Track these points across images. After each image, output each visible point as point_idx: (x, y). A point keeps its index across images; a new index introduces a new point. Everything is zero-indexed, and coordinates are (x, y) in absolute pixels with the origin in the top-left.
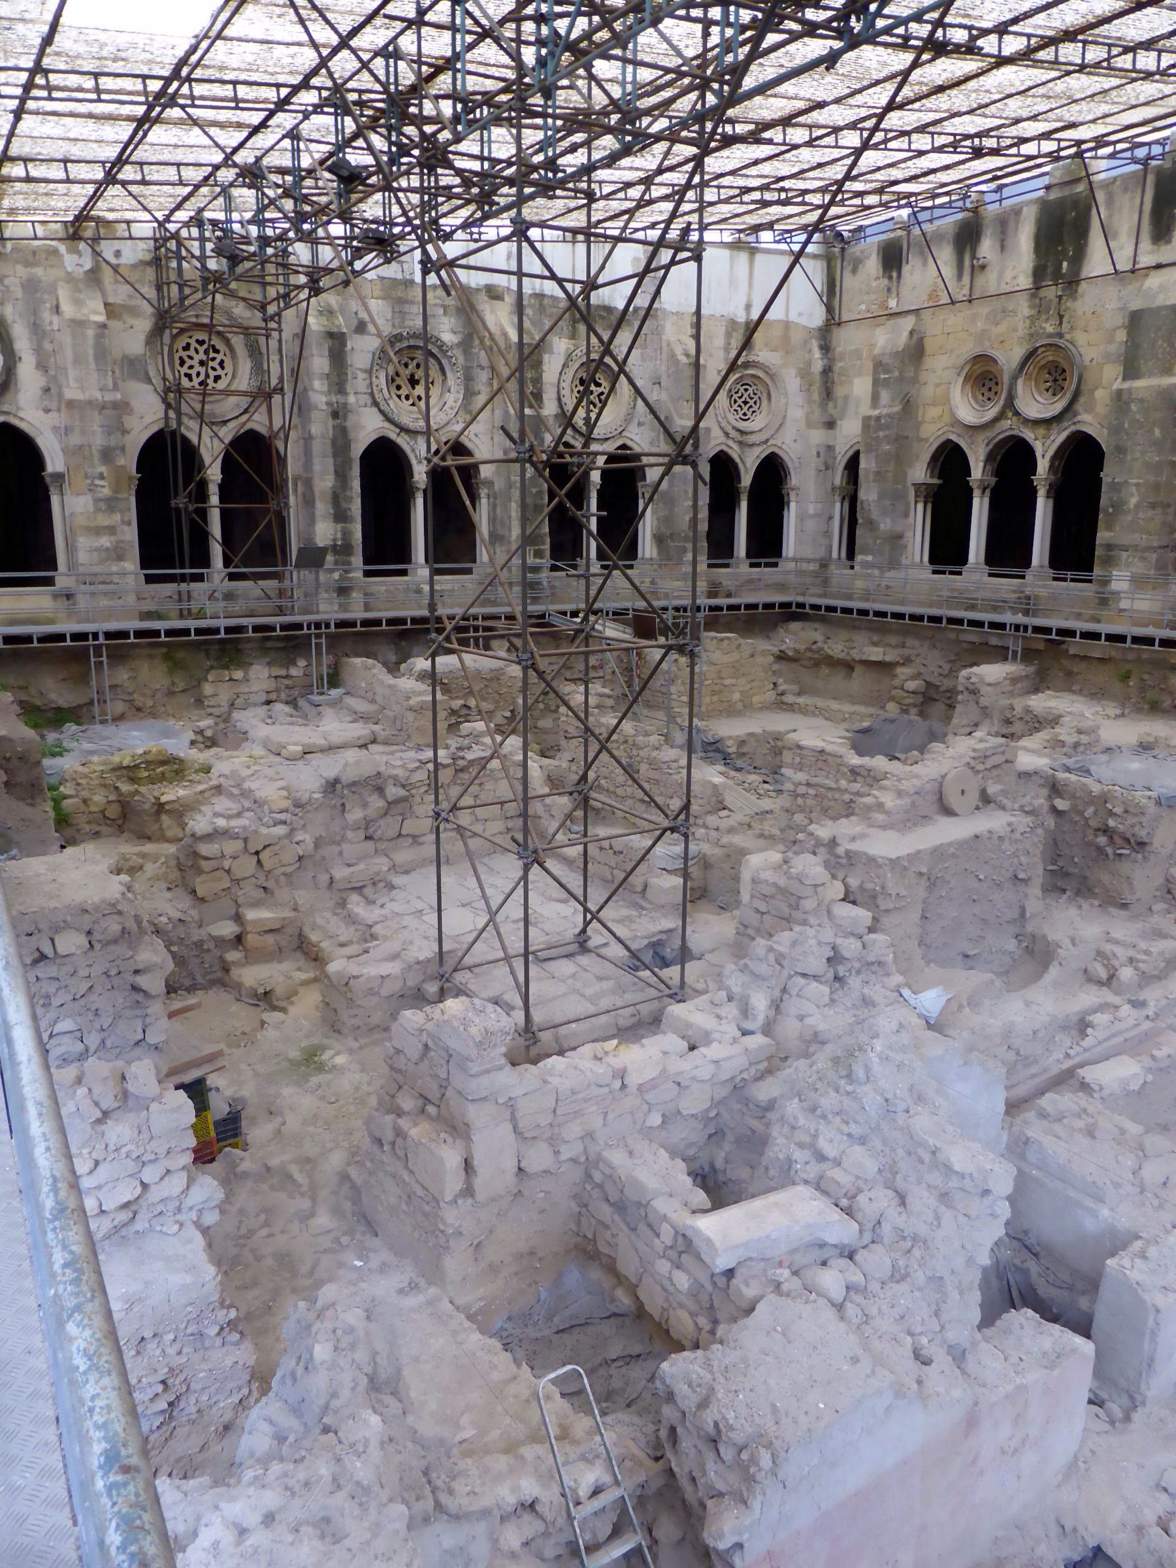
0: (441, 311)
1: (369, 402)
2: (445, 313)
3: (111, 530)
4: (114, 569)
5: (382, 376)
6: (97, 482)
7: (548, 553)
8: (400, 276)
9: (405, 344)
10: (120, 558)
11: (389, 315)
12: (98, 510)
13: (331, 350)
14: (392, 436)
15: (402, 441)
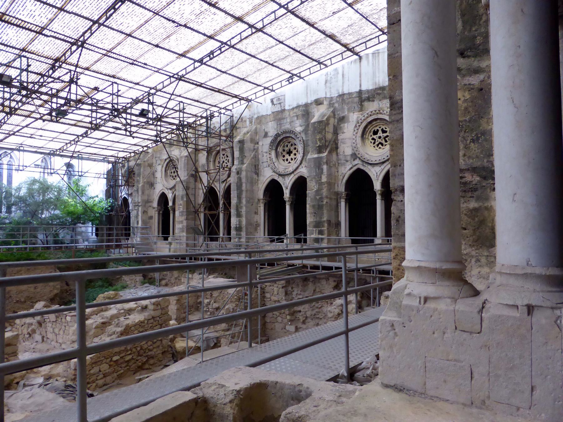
0: (296, 118)
1: (268, 166)
2: (297, 119)
3: (182, 222)
4: (182, 235)
5: (273, 153)
6: (180, 206)
7: (326, 232)
8: (280, 109)
9: (282, 137)
10: (183, 231)
11: (276, 127)
12: (180, 215)
13: (240, 148)
14: (276, 177)
15: (280, 180)
